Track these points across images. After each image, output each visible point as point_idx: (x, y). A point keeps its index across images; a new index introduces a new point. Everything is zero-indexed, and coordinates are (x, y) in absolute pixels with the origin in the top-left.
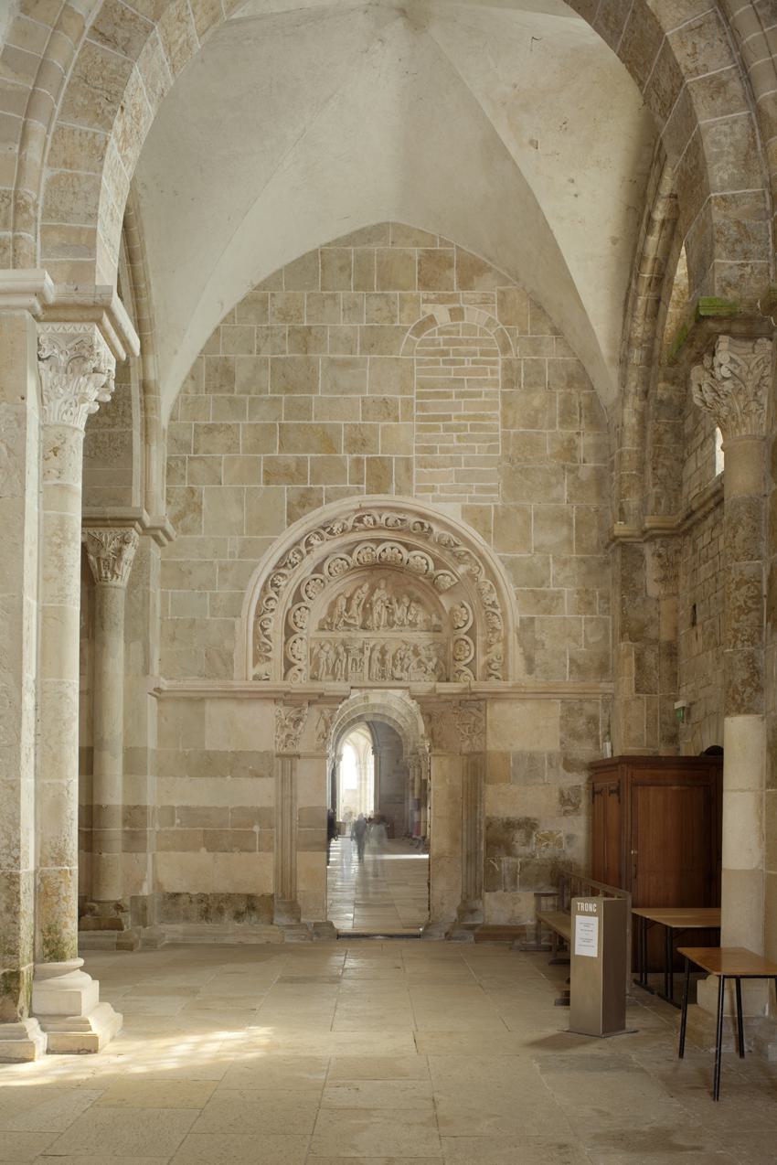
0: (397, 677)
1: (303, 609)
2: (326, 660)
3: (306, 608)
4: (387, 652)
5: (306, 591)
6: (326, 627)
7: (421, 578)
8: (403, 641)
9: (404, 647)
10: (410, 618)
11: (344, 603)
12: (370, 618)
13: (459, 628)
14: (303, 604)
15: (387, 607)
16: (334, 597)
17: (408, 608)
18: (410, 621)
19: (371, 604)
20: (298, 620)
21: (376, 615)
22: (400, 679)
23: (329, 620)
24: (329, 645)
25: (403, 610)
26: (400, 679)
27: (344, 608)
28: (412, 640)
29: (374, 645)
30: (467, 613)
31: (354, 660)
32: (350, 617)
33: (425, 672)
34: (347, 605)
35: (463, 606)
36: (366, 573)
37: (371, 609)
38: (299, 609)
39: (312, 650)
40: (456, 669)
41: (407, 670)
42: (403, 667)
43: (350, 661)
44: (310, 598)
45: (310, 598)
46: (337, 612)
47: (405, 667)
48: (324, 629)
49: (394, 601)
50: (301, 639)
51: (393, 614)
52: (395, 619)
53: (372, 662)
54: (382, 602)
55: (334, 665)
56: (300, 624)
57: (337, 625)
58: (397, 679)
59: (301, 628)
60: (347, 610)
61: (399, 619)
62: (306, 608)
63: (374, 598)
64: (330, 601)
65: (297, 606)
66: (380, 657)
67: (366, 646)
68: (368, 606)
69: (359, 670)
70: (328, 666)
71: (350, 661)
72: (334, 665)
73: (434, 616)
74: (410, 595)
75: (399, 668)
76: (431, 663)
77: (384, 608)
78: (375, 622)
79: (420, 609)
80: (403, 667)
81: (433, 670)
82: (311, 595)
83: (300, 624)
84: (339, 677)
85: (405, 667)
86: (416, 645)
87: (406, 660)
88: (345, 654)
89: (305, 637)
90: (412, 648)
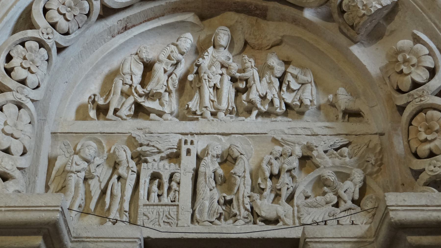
0: (263, 214)
1: (35, 45)
2: (86, 179)
3: (42, 44)
4: (235, 159)
5: (45, 11)
6: (93, 113)
7: (308, 14)
8: (275, 141)
9: (278, 149)
10: (289, 98)
11: (138, 70)
12: (196, 97)
13: (416, 85)
14: (30, 33)
15: (234, 80)
16: (115, 63)
17: (281, 80)
18: (287, 105)
19: (197, 73)
20: (16, 62)
21: (208, 93)
22: (276, 221)
23: (101, 101)
24: (94, 145)
25: (270, 83)
26: (276, 221)
27: (137, 79)
28: (292, 138)
29: (205, 152)
30: (431, 54)
31: (155, 176)
32: (149, 96)
33: (337, 205)
34: (144, 76)
35: (417, 40)
36: (190, 17)
37: (199, 79)
38: (23, 44)
39: (52, 161)
40: (424, 177)
41: (290, 199)
42: (278, 196)
43: (145, 179)
44: (54, 25)
45: (54, 25)
46: (119, 85)
47: (285, 194)
48: (92, 119)
49: (250, 62)
50: (20, 106)
51: (246, 90)
52: (254, 96)
53: (201, 179)
54: (223, 66)
55: (104, 192)
56: (21, 73)
57: (116, 111)
58: (267, 221)
59: (23, 82)
60: (143, 84)
61: (263, 98)
62: (42, 44)
63: (205, 62)
64: (106, 70)
65: (20, 36)
66: (220, 171)
67: (184, 148)
68: (191, 77)
69: (166, 200)
70: (88, 195)
71: (145, 179)
72: (104, 192)
73: (341, 91)
74: (287, 63)
75: (269, 195)
76: (348, 184)
77: (227, 78)
78: (207, 103)
79: (309, 78)
80: (278, 196)
81: (353, 201)
82: (59, 19)
83: (21, 73)
84: (114, 214)
85: (285, 194)
86: (309, 148)
87: (285, 178)
88: (133, 164)
89: (30, 105)
90: (298, 151)
